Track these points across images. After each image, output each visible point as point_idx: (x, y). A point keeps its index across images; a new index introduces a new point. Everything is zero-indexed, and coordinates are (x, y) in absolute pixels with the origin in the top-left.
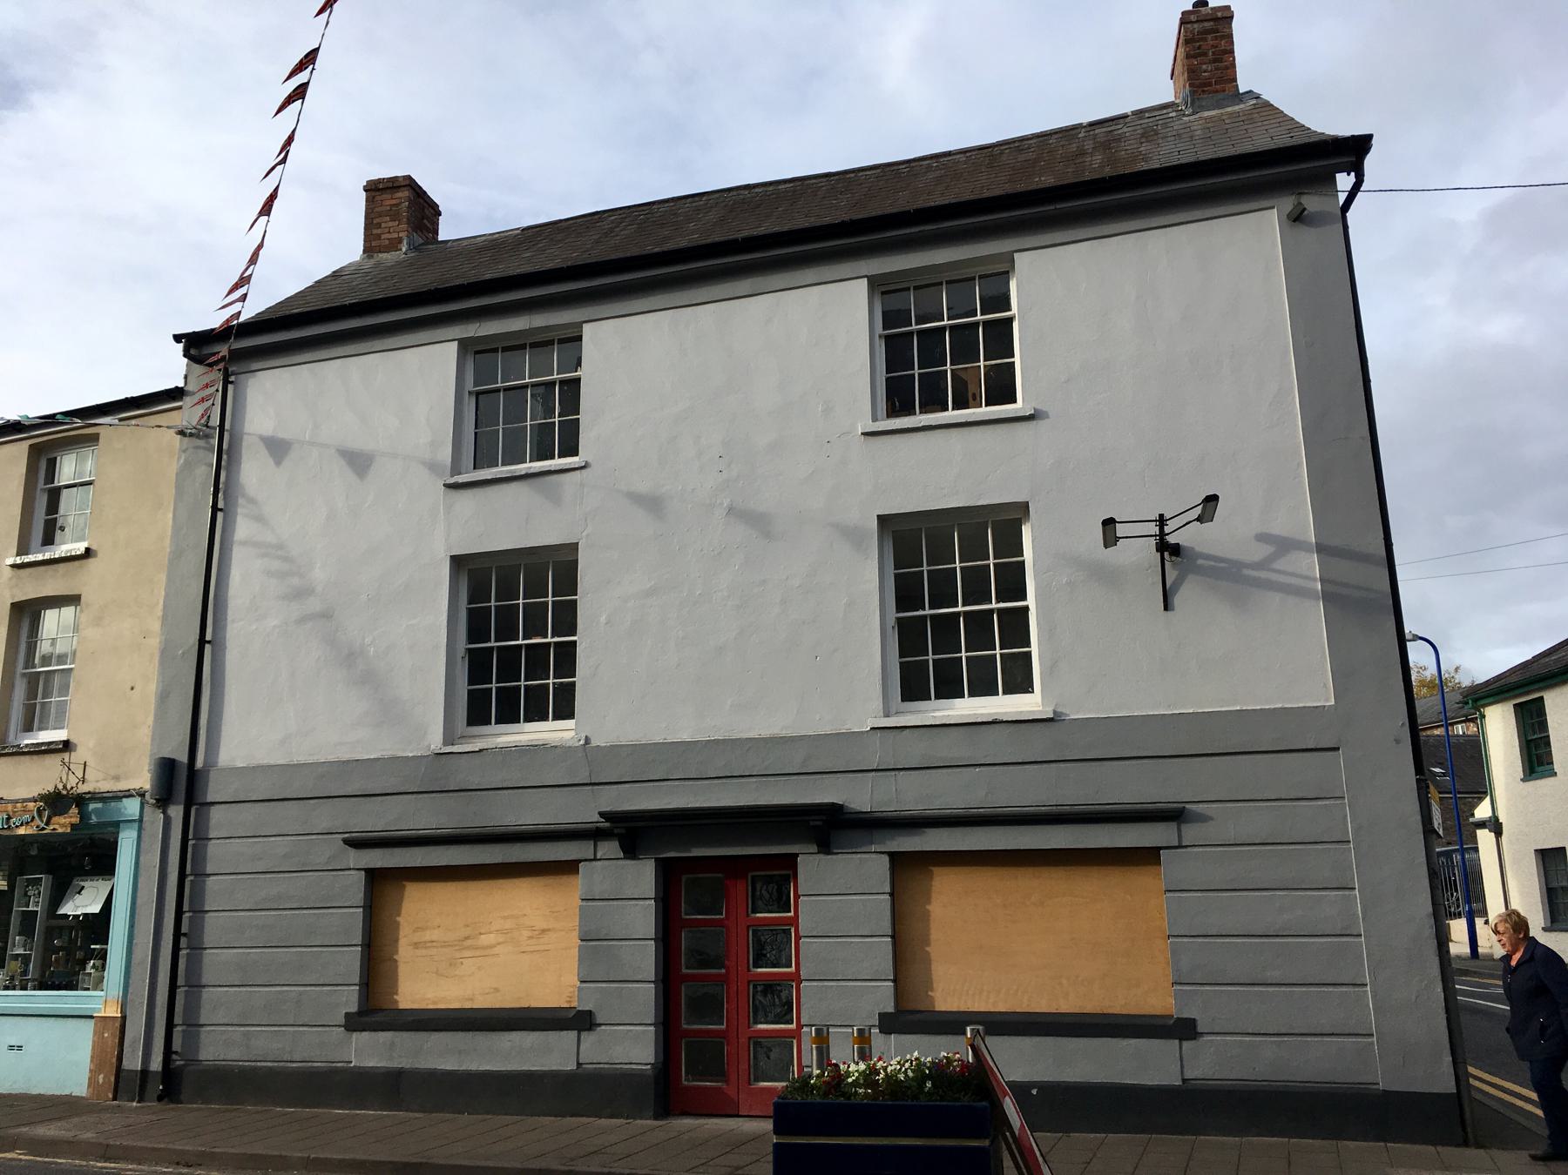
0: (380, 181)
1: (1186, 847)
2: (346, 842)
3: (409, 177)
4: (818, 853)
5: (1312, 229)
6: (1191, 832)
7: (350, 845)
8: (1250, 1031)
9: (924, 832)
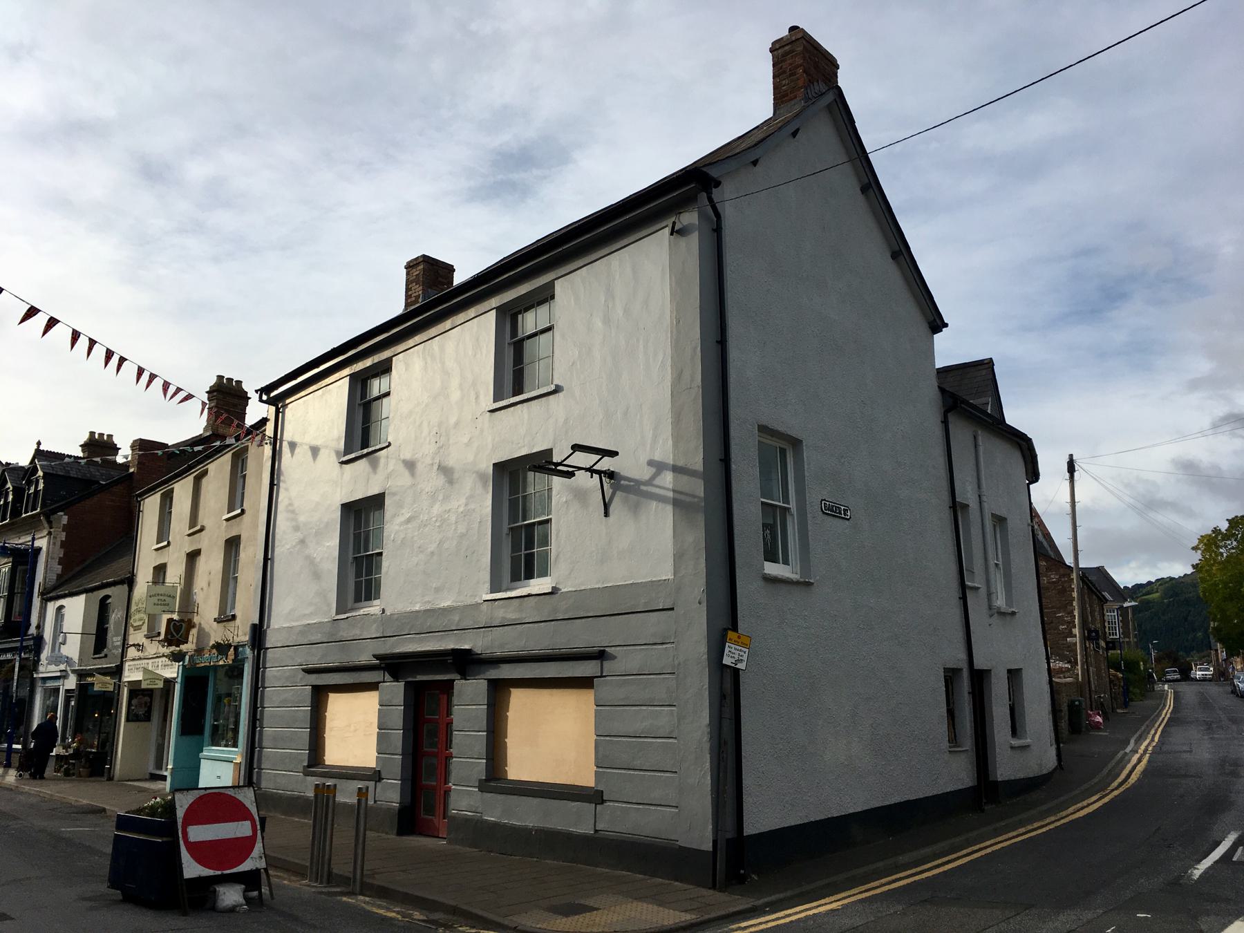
0: (411, 261)
1: (605, 676)
2: (304, 670)
3: (424, 256)
4: (461, 679)
5: (684, 238)
6: (607, 665)
7: (305, 672)
8: (625, 800)
9: (500, 667)
